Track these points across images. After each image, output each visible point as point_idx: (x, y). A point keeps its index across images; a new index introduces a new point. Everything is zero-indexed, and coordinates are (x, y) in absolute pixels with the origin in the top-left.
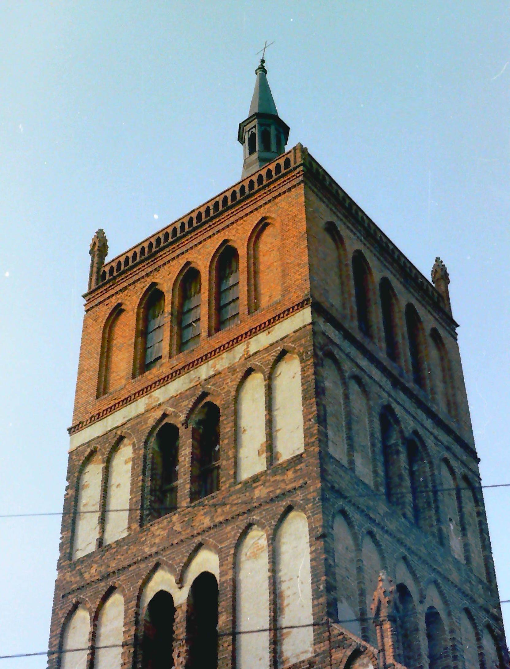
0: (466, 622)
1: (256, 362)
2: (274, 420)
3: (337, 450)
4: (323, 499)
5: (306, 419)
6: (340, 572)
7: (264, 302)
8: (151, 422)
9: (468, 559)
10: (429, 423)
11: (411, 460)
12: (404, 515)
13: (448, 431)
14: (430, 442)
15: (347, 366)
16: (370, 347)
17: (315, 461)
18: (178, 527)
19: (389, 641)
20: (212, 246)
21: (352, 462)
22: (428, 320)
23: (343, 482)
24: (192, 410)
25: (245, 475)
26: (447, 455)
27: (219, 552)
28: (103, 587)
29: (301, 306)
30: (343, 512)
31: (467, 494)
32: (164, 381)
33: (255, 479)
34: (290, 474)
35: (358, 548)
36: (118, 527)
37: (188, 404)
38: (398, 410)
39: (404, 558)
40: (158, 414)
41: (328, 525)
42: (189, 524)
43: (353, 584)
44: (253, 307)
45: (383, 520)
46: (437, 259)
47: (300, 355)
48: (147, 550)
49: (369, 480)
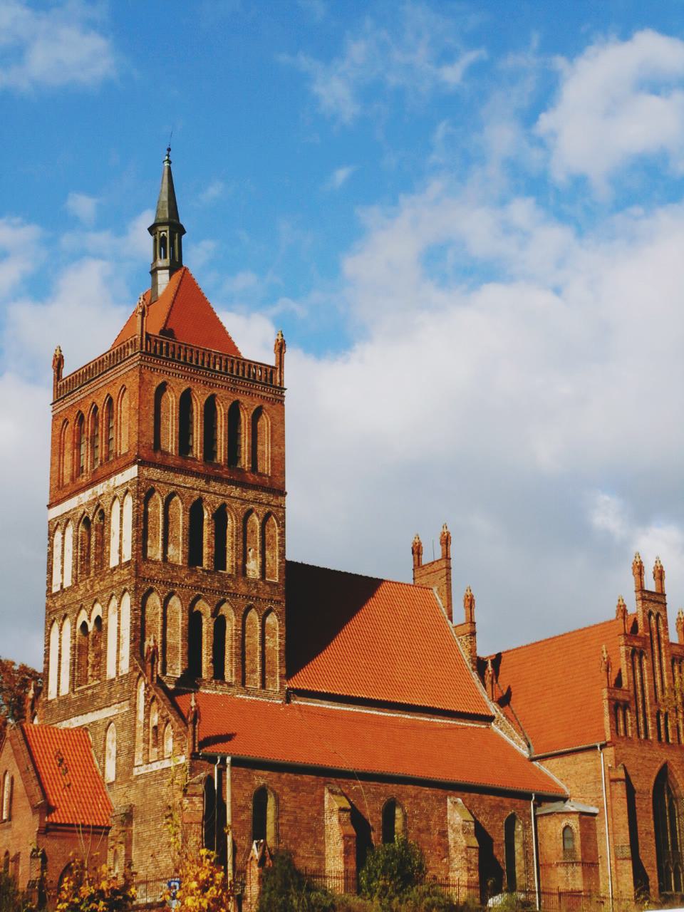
18: (88, 587)
25: (112, 566)
28: (62, 613)
29: (134, 463)
33: (115, 568)
36: (68, 583)
37: (93, 508)
45: (184, 581)
48: (79, 598)
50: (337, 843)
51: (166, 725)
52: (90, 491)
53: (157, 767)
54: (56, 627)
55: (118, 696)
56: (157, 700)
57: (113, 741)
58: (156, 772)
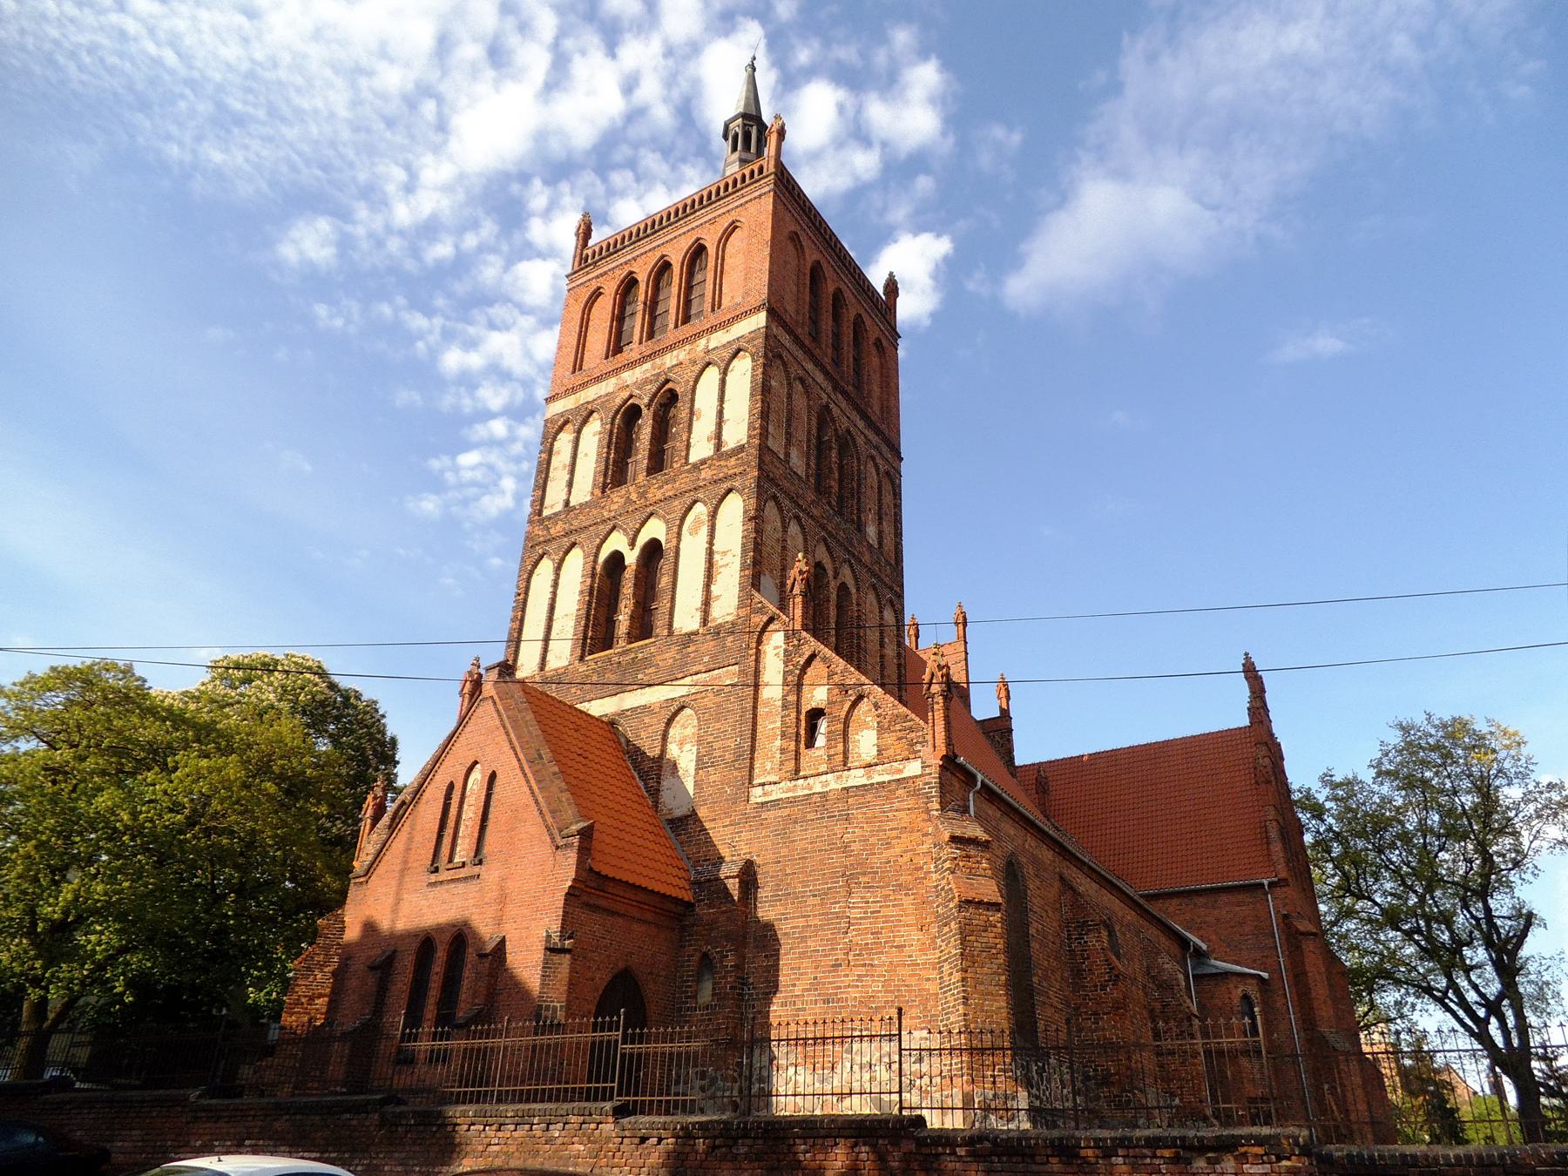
0: (871, 597)
1: (713, 357)
2: (725, 409)
3: (777, 444)
4: (759, 486)
5: (751, 414)
6: (766, 550)
7: (725, 302)
8: (618, 401)
9: (880, 543)
10: (861, 424)
11: (840, 455)
12: (829, 503)
13: (878, 432)
14: (860, 441)
15: (795, 370)
16: (817, 352)
17: (754, 452)
18: (634, 497)
19: (798, 612)
20: (685, 243)
21: (787, 455)
22: (873, 330)
23: (778, 472)
24: (655, 395)
25: (694, 457)
26: (874, 452)
27: (667, 522)
28: (566, 542)
30: (774, 498)
31: (887, 487)
32: (631, 365)
33: (703, 462)
34: (733, 461)
35: (785, 528)
36: (583, 491)
38: (836, 411)
39: (825, 540)
40: (625, 394)
41: (760, 509)
42: (642, 495)
43: (776, 560)
44: (716, 305)
46: (891, 274)
47: (752, 356)
49: (801, 472)
50: (1103, 988)
51: (854, 704)
52: (647, 366)
53: (833, 783)
54: (546, 567)
55: (706, 659)
56: (824, 659)
57: (681, 744)
58: (823, 795)
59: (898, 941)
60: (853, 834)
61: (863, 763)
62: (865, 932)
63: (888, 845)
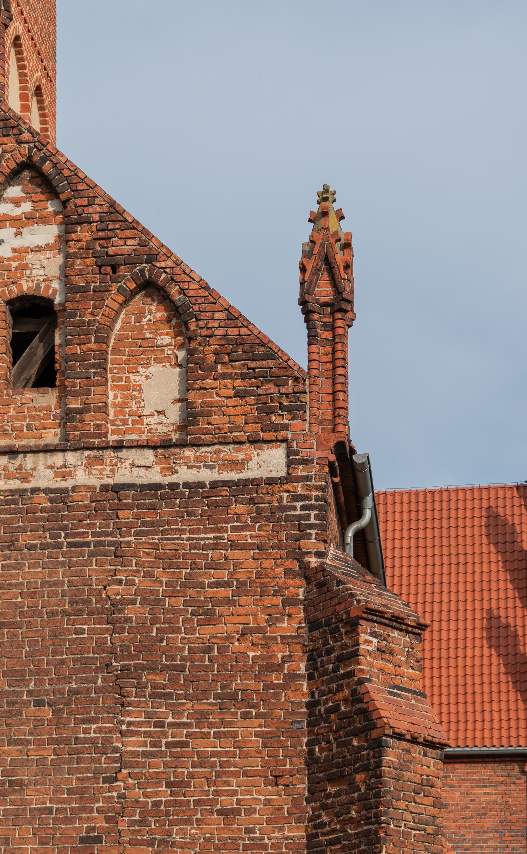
58: (60, 496)
59: (228, 802)
60: (128, 584)
61: (157, 440)
62: (156, 779)
63: (210, 618)
